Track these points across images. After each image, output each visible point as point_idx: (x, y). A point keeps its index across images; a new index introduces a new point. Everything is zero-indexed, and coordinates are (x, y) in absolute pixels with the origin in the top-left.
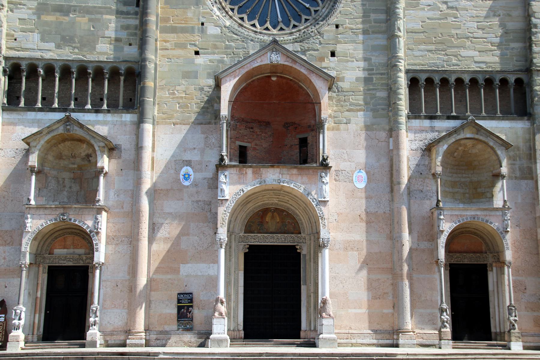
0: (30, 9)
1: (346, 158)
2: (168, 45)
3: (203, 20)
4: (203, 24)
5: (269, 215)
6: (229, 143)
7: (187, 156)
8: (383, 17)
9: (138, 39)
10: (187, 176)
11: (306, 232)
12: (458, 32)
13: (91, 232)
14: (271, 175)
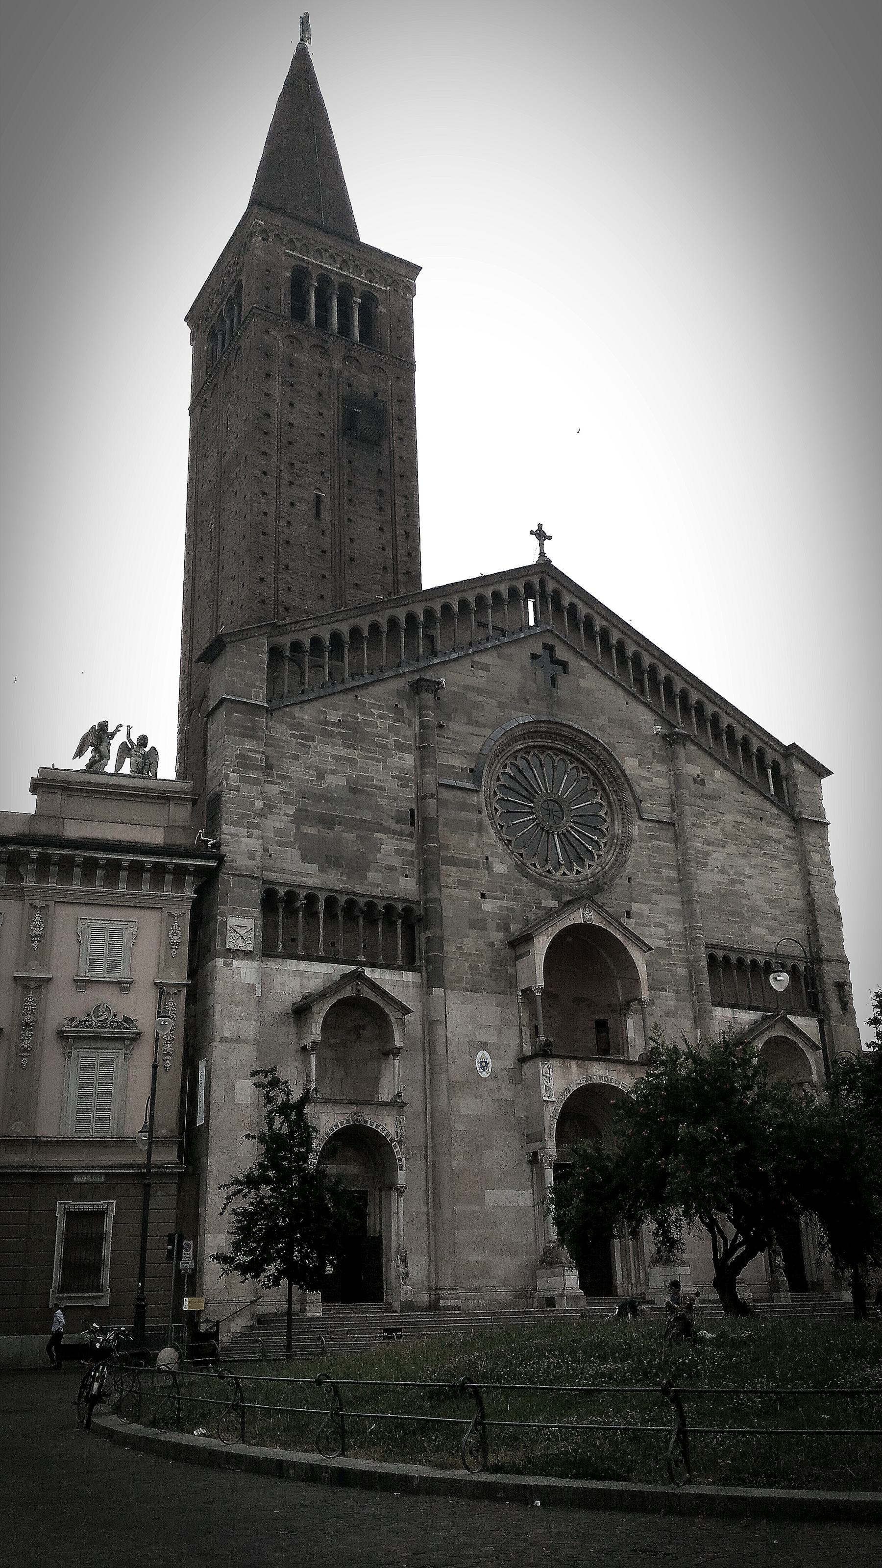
0: (285, 814)
2: (450, 881)
3: (488, 854)
4: (487, 858)
7: (483, 1037)
8: (674, 874)
9: (416, 869)
10: (484, 1064)
12: (747, 902)
13: (392, 1140)
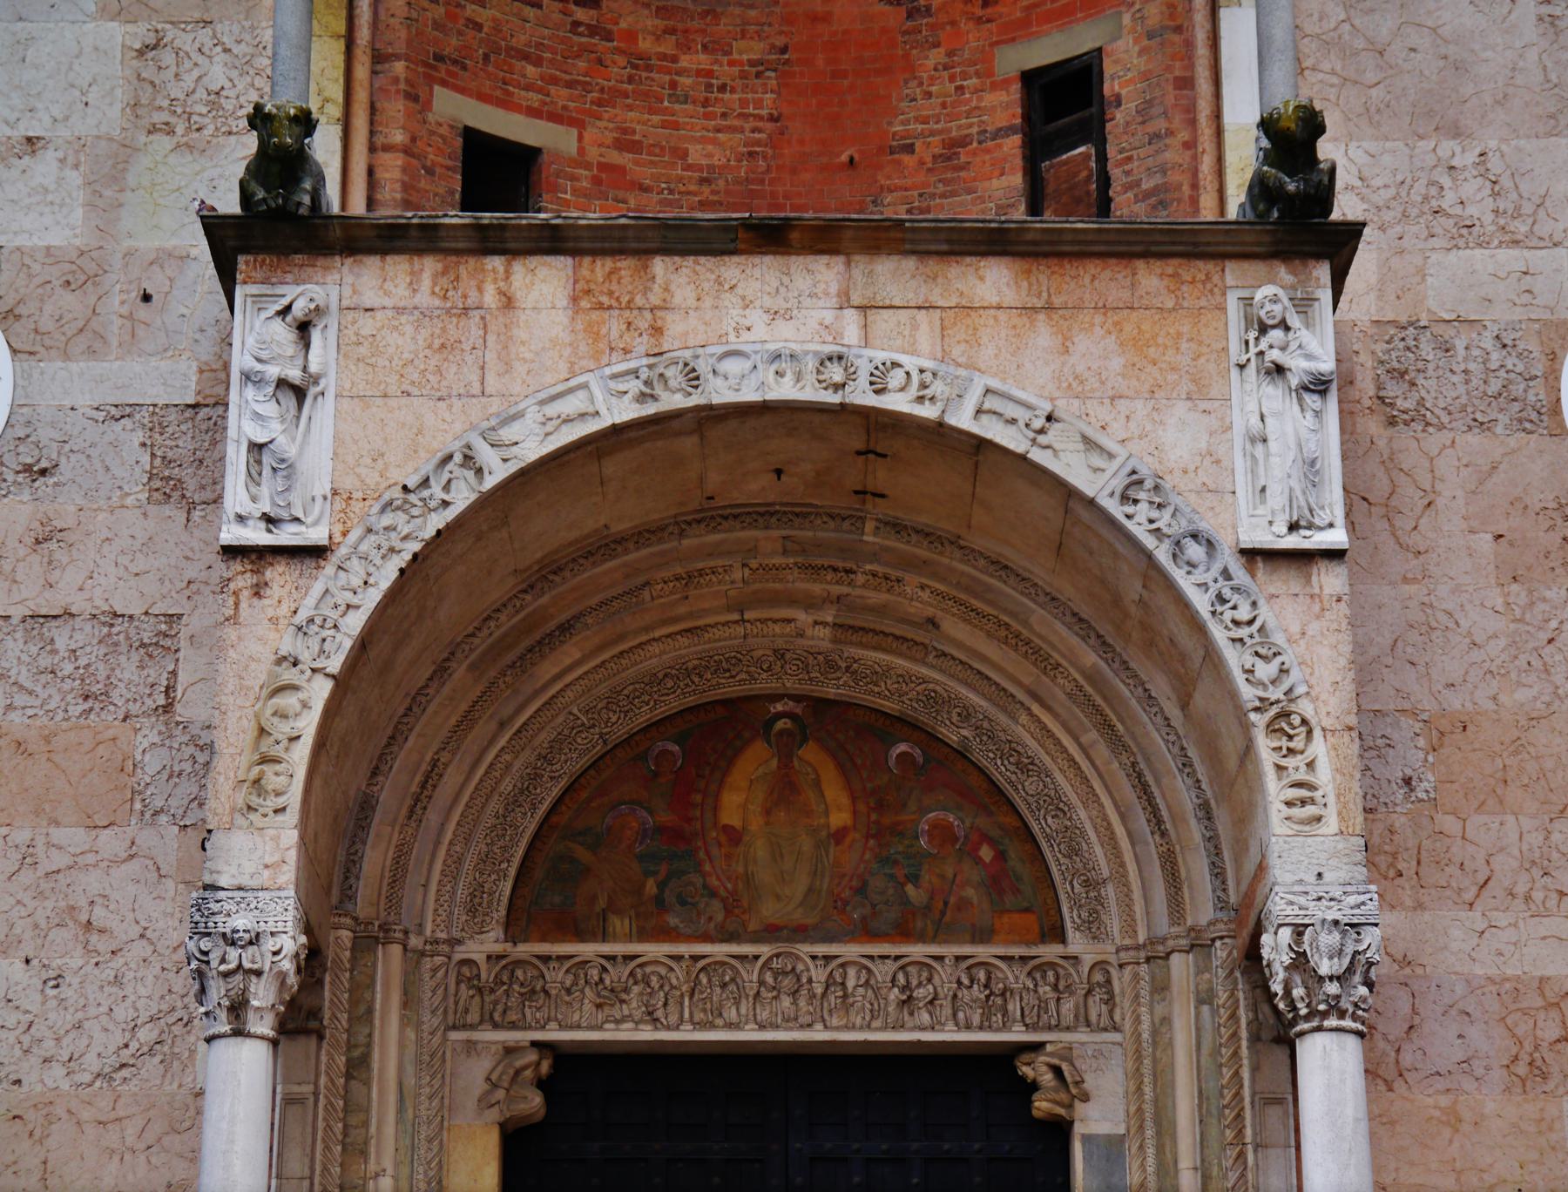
1: (1480, 209)
5: (756, 762)
6: (361, 96)
11: (1114, 924)
14: (756, 317)
